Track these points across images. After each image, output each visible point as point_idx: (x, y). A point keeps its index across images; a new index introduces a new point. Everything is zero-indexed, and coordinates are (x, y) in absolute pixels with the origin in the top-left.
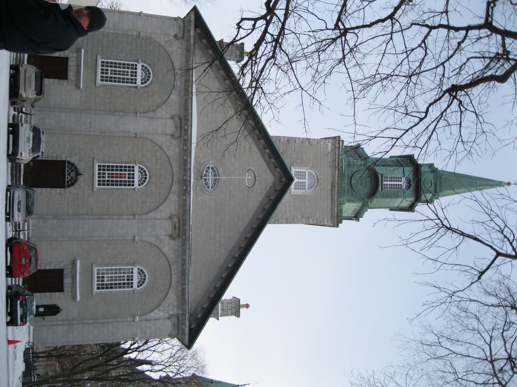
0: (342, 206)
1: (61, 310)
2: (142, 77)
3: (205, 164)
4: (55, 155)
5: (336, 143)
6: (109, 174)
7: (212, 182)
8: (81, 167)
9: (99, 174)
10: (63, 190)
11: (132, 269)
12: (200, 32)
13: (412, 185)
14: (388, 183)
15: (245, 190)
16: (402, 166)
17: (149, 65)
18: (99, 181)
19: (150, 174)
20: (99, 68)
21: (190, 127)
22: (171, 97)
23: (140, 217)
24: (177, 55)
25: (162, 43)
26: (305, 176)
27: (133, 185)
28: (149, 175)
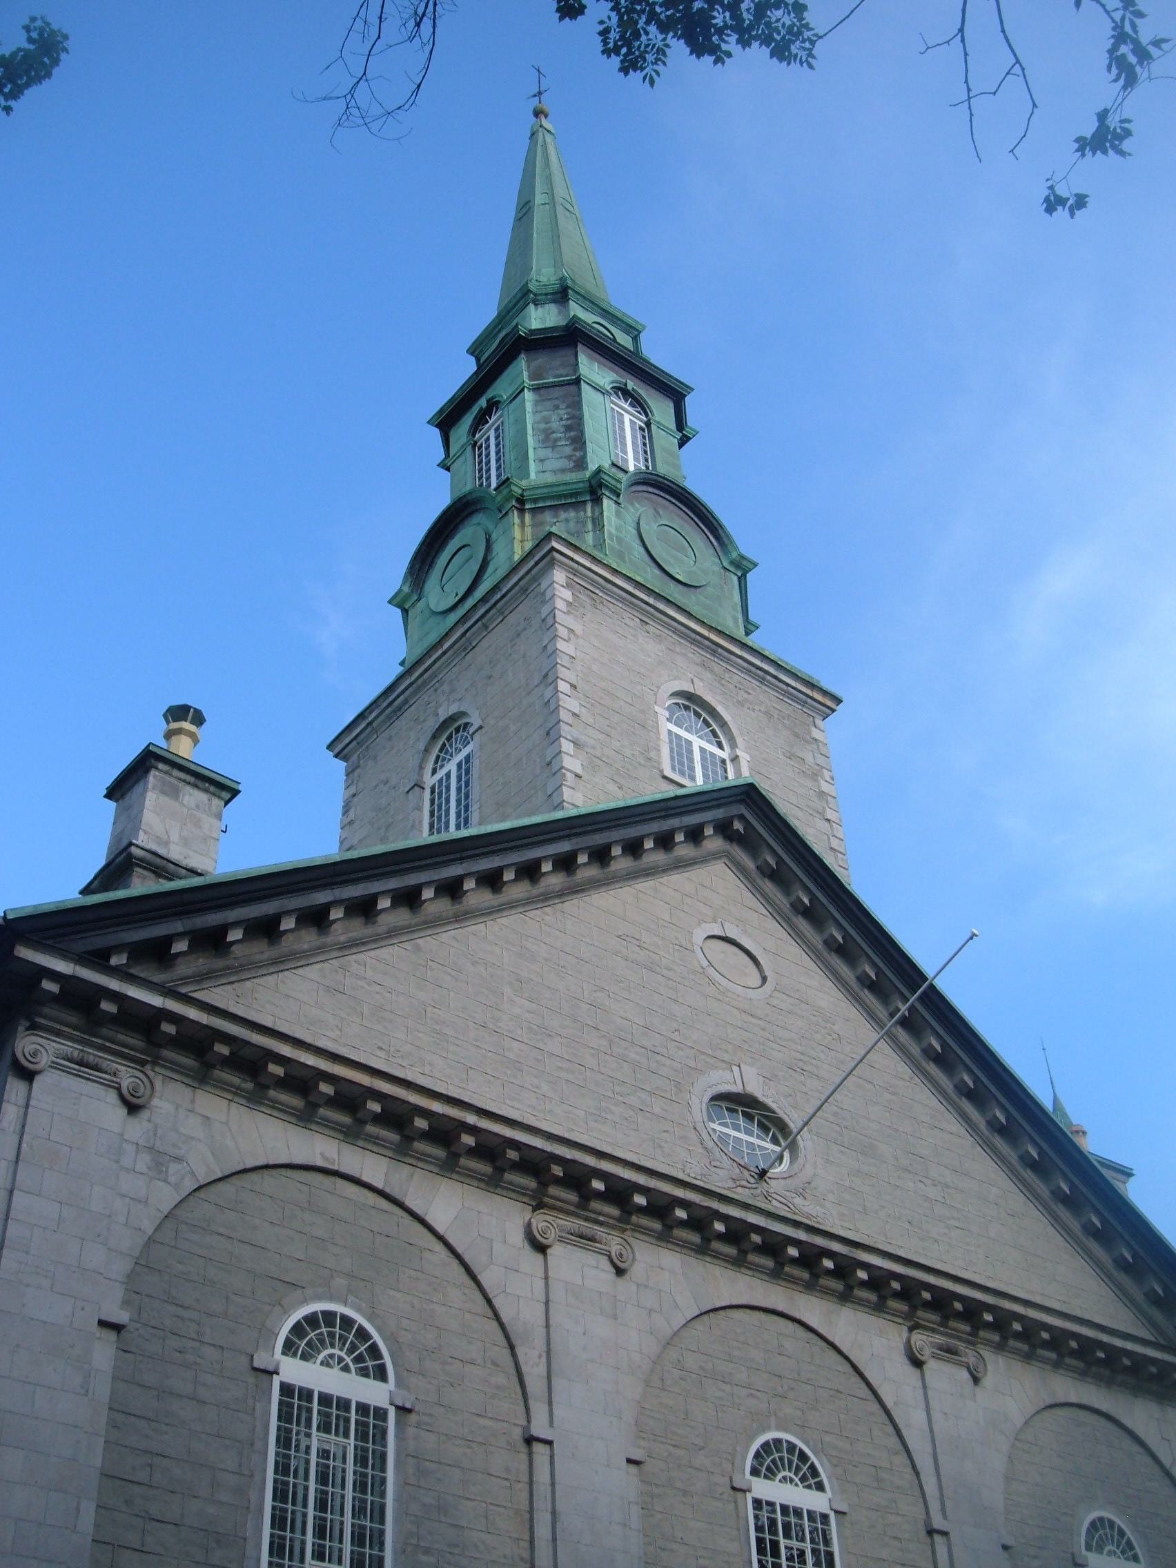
21: (605, 1166)
22: (440, 1229)
23: (934, 1506)
24: (226, 1123)
25: (166, 1197)
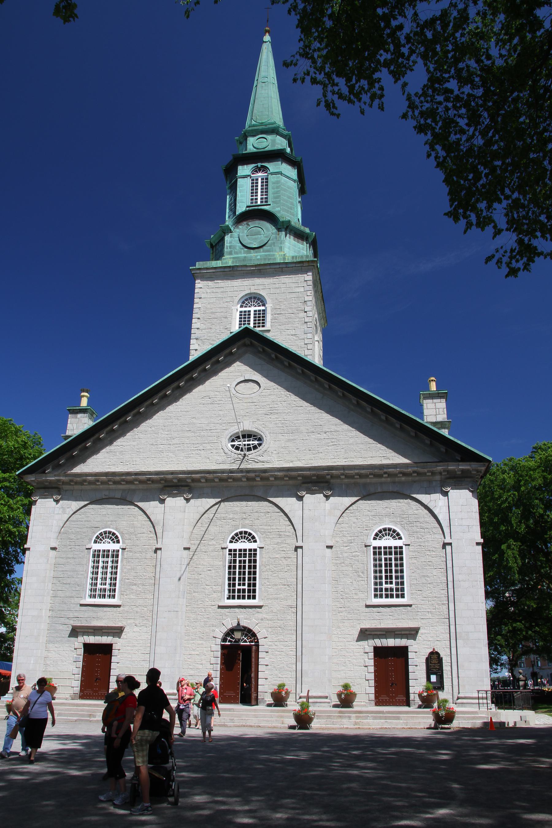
0: (287, 258)
1: (434, 649)
2: (109, 543)
3: (227, 451)
4: (213, 660)
5: (200, 273)
6: (239, 585)
7: (253, 441)
8: (230, 623)
9: (239, 598)
10: (261, 649)
11: (375, 548)
12: (51, 467)
13: (263, 164)
14: (259, 197)
15: (263, 394)
16: (236, 181)
17: (95, 533)
18: (249, 597)
19: (240, 527)
20: (98, 601)
23: (300, 538)
24: (81, 496)
26: (245, 312)
27: (255, 550)
28: (242, 528)
